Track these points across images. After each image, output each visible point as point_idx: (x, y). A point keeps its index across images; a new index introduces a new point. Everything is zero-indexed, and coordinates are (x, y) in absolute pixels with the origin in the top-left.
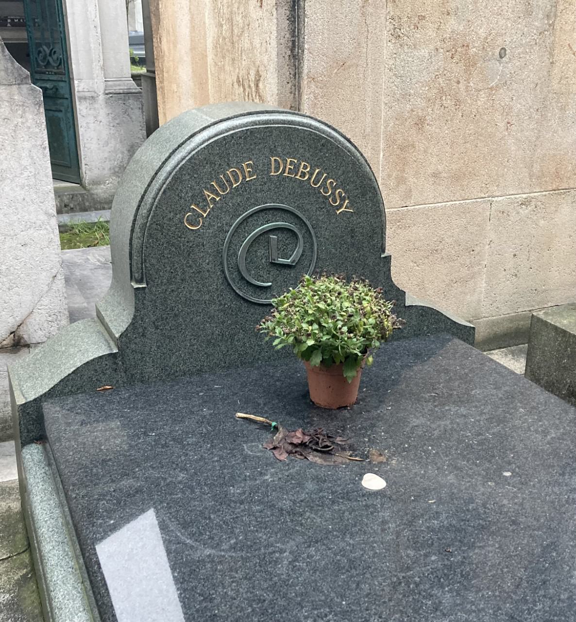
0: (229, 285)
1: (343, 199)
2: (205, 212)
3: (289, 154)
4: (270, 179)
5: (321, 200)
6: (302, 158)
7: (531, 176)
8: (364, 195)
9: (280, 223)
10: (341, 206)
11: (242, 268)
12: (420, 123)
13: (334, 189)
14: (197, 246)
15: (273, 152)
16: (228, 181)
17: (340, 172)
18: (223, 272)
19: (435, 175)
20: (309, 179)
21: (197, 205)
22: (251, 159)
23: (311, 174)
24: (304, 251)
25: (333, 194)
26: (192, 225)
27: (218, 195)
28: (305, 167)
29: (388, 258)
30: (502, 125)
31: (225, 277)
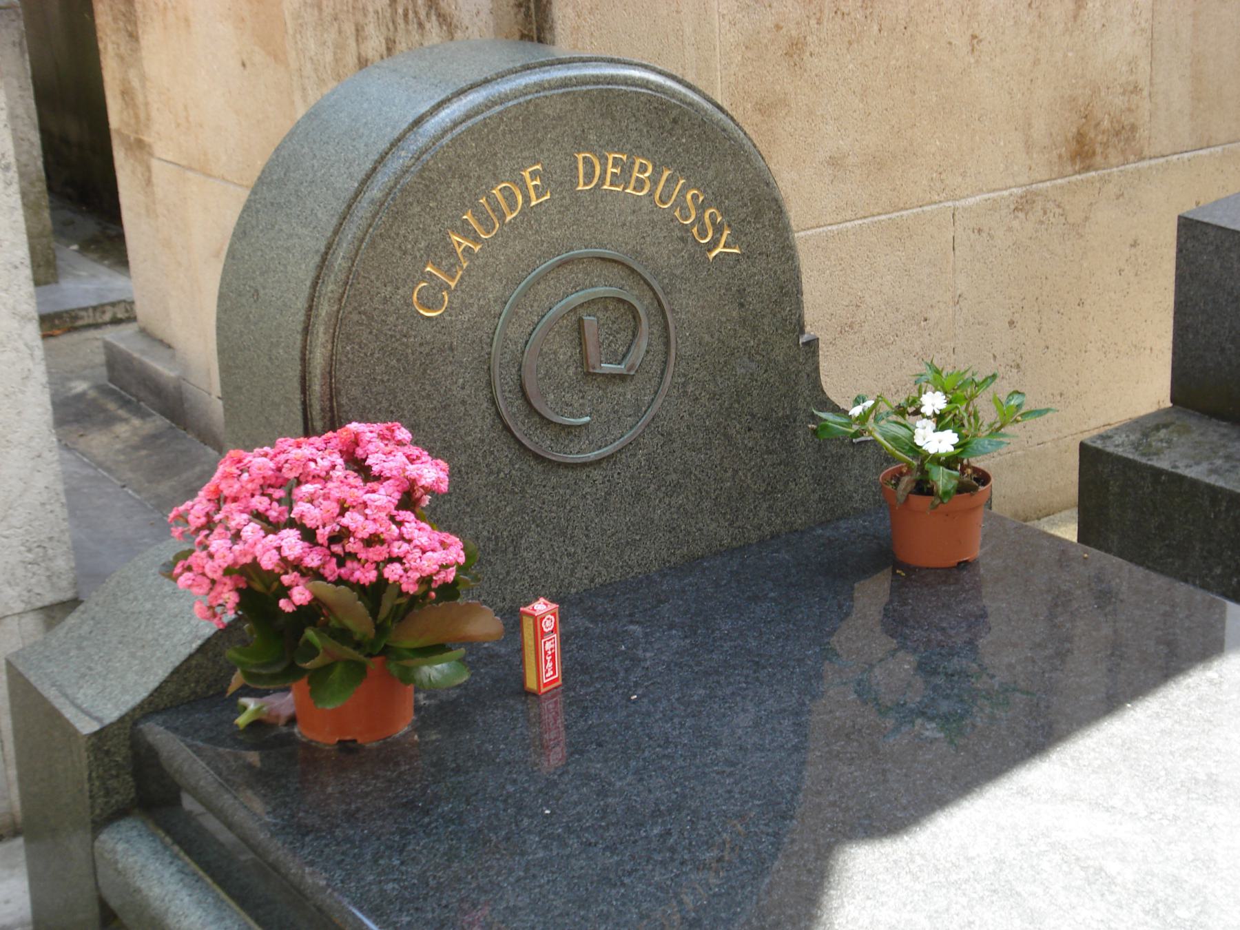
0: (507, 428)
1: (718, 229)
2: (453, 278)
3: (612, 145)
4: (576, 197)
5: (677, 233)
6: (638, 150)
7: (1028, 147)
8: (758, 215)
9: (601, 291)
10: (714, 243)
11: (531, 389)
12: (795, 48)
13: (701, 208)
14: (441, 351)
15: (580, 142)
16: (496, 209)
17: (711, 174)
18: (493, 402)
19: (834, 162)
20: (651, 194)
21: (438, 266)
22: (537, 162)
23: (654, 181)
24: (649, 345)
25: (700, 219)
26: (429, 308)
27: (477, 239)
28: (643, 169)
29: (813, 344)
30: (961, 42)
31: (498, 414)
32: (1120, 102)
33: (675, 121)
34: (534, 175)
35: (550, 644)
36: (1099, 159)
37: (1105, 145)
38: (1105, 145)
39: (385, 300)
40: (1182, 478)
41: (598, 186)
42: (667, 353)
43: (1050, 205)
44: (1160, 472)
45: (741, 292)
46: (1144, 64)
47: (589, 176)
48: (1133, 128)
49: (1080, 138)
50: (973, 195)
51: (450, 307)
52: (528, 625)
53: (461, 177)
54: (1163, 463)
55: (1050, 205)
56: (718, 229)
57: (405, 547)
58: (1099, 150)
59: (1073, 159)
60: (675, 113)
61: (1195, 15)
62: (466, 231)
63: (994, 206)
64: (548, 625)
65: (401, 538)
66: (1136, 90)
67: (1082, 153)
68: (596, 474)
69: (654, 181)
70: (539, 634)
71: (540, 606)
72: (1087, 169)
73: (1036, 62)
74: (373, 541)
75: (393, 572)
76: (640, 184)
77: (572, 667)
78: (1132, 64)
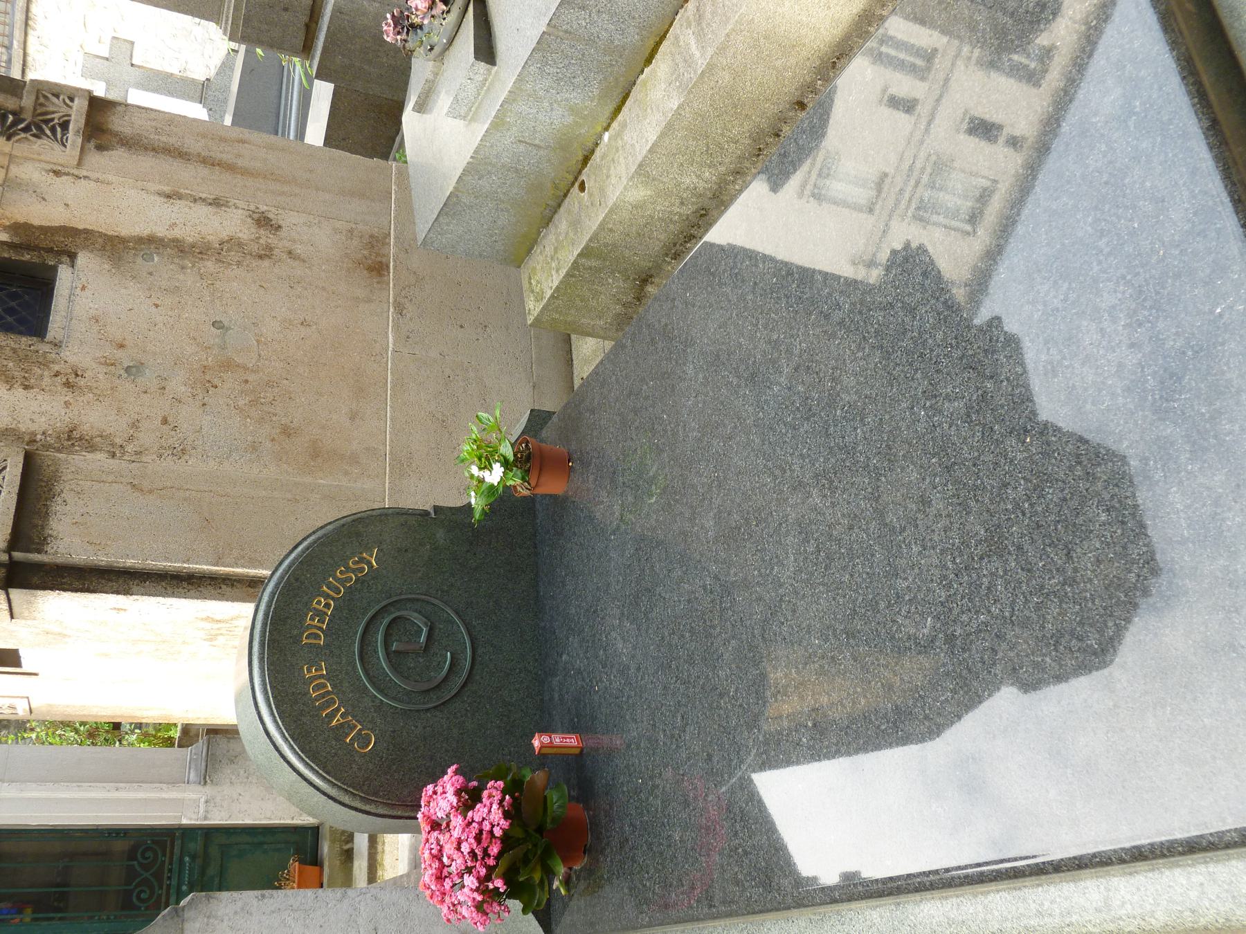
0: (443, 704)
1: (362, 560)
2: (355, 727)
3: (303, 620)
4: (327, 645)
5: (359, 586)
6: (307, 605)
7: (369, 301)
8: (358, 534)
9: (380, 637)
10: (369, 563)
11: (426, 686)
12: (287, 431)
13: (348, 568)
14: (394, 738)
15: (297, 640)
16: (323, 696)
17: (330, 561)
18: (428, 710)
19: (353, 417)
20: (333, 599)
21: (348, 735)
22: (302, 668)
23: (327, 596)
24: (416, 611)
25: (354, 571)
26: (369, 743)
27: (338, 710)
28: (319, 603)
29: (437, 509)
30: (304, 331)
31: (435, 707)
32: (355, 242)
33: (297, 580)
34: (309, 671)
35: (557, 739)
36: (384, 260)
37: (378, 255)
38: (378, 255)
39: (360, 769)
40: (557, 287)
41: (323, 631)
42: (423, 601)
43: (403, 293)
44: (552, 296)
45: (399, 550)
46: (338, 224)
47: (317, 637)
48: (372, 236)
49: (370, 269)
50: (387, 337)
51: (371, 730)
52: (544, 751)
53: (302, 715)
54: (549, 293)
55: (403, 293)
56: (362, 560)
57: (486, 822)
58: (379, 259)
59: (381, 275)
60: (292, 580)
61: (317, 189)
62: (331, 716)
63: (397, 327)
64: (546, 739)
65: (480, 823)
66: (351, 231)
67: (378, 269)
68: (480, 651)
69: (327, 596)
70: (551, 745)
71: (536, 743)
72: (388, 267)
73: (324, 289)
74: (478, 838)
75: (498, 832)
76: (327, 606)
77: (573, 729)
78: (336, 231)
